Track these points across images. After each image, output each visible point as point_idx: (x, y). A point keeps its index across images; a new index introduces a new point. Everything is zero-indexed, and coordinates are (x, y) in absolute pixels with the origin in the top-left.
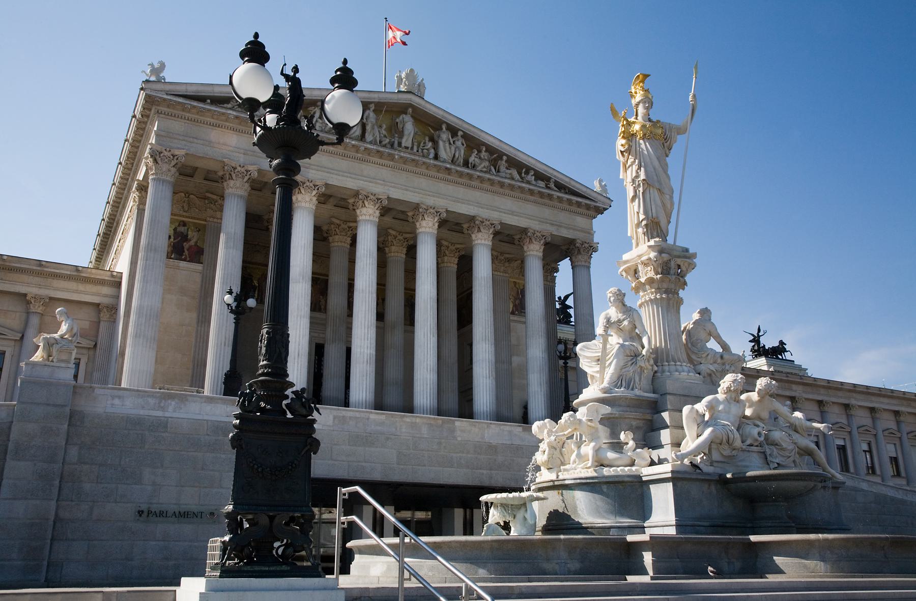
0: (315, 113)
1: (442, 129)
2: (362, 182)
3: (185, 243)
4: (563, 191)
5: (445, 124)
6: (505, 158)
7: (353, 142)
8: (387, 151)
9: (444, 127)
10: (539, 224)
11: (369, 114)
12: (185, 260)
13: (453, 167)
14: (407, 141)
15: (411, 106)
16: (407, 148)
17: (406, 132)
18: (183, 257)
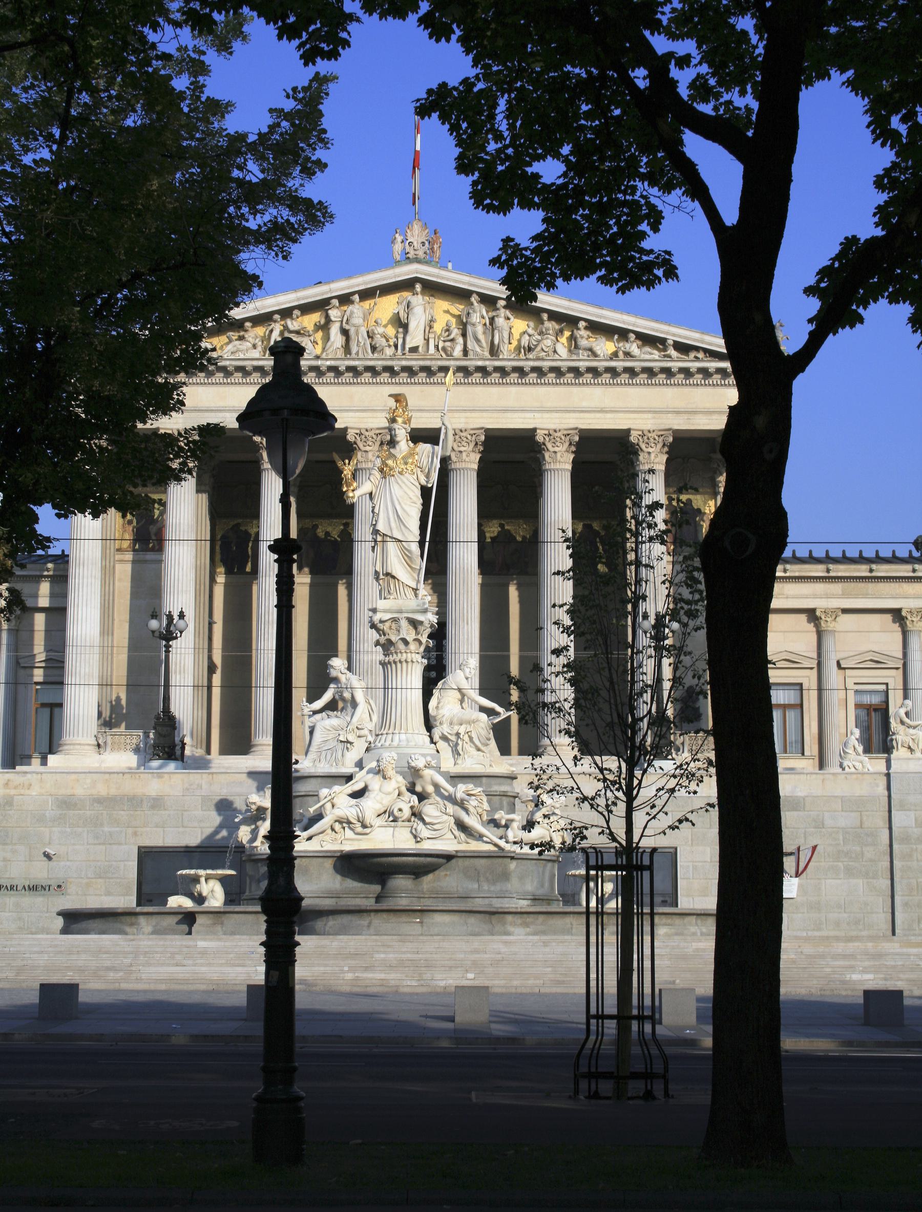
0: (271, 331)
1: (472, 304)
2: (351, 414)
3: (151, 527)
4: (692, 355)
5: (474, 295)
6: (582, 324)
7: (328, 363)
8: (380, 363)
9: (473, 299)
10: (654, 418)
11: (352, 313)
12: (152, 550)
13: (487, 363)
14: (415, 338)
15: (416, 280)
16: (414, 350)
17: (412, 327)
18: (151, 545)
